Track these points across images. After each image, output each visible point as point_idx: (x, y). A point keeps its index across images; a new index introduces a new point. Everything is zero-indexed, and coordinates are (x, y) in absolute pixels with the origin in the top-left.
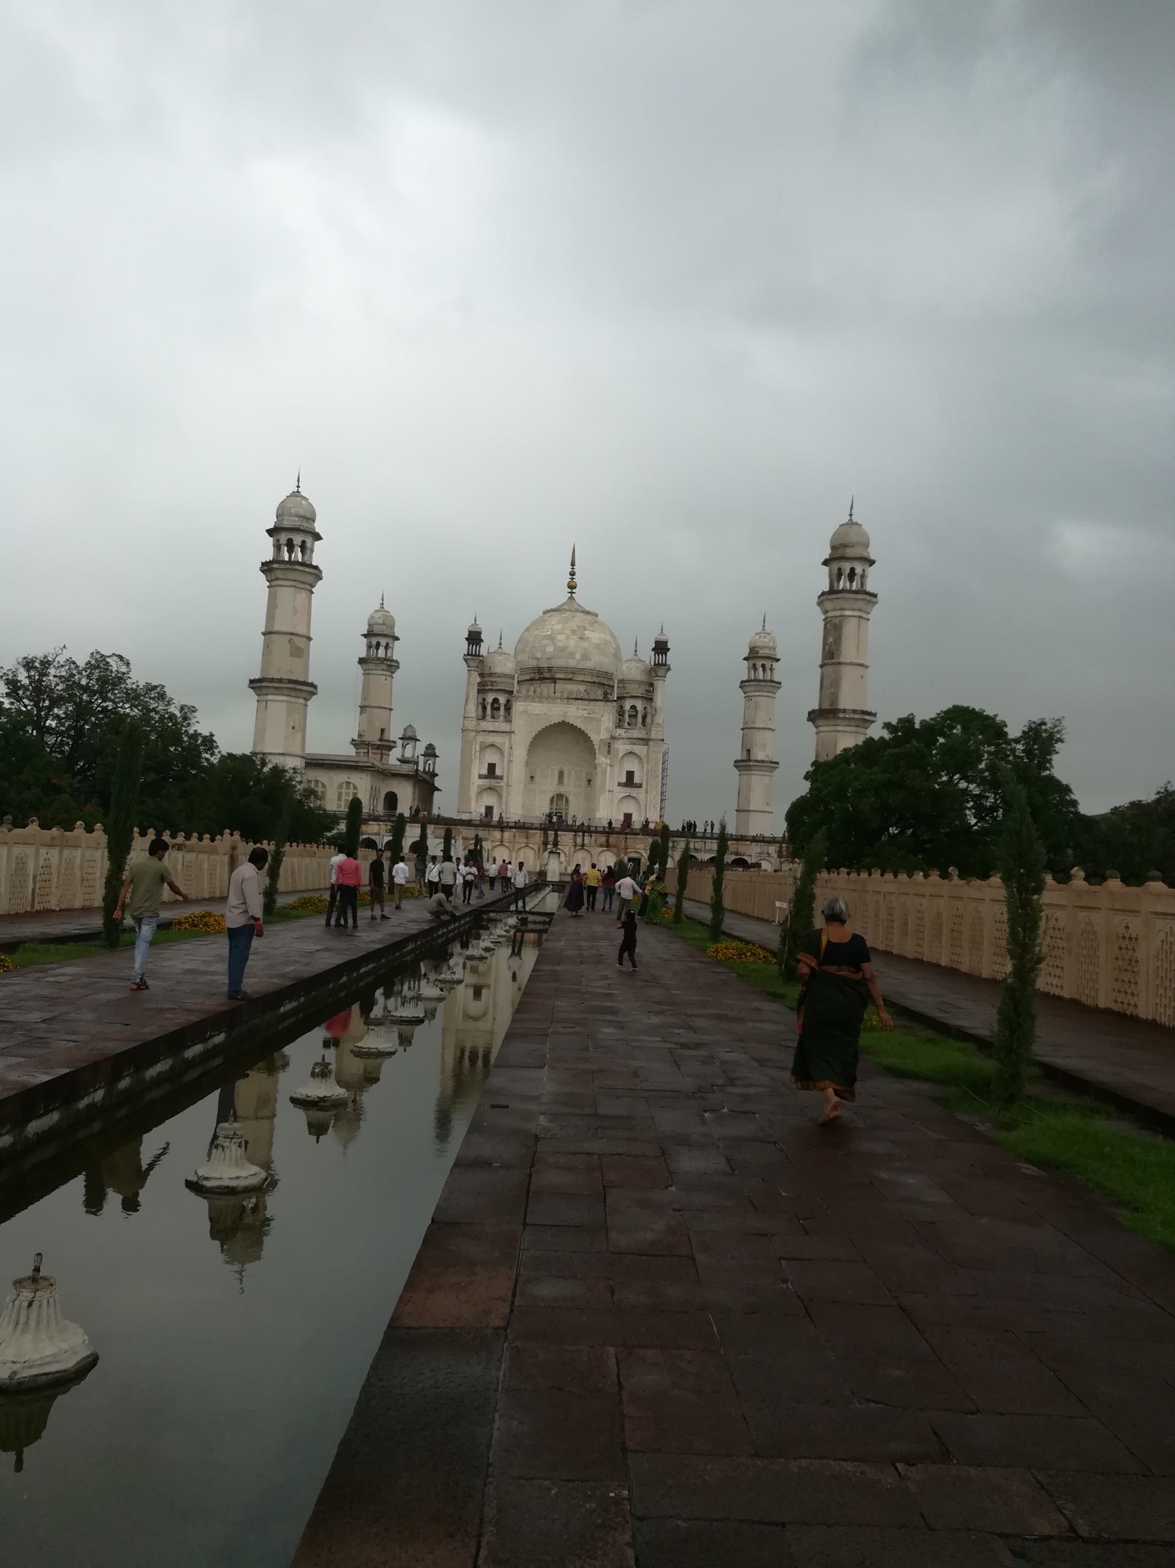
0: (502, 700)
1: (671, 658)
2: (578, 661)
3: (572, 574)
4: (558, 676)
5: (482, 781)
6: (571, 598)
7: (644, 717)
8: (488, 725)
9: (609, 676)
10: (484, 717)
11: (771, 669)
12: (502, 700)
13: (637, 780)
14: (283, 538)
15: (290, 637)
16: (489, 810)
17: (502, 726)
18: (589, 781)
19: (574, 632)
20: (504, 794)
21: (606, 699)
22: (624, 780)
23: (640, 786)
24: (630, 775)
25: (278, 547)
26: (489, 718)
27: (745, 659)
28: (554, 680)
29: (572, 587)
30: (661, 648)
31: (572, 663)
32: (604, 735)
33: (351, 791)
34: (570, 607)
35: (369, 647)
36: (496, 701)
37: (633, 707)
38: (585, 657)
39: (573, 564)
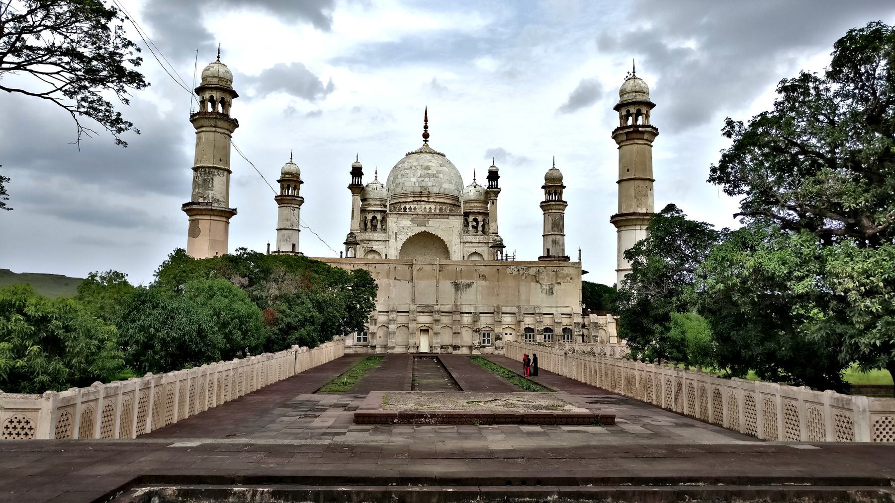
0: (379, 217)
1: (501, 183)
3: (426, 127)
6: (426, 145)
9: (456, 199)
11: (561, 194)
12: (379, 217)
14: (207, 95)
17: (377, 236)
25: (203, 103)
26: (369, 230)
27: (543, 187)
29: (426, 136)
30: (493, 176)
34: (426, 150)
35: (282, 188)
36: (374, 218)
39: (426, 120)
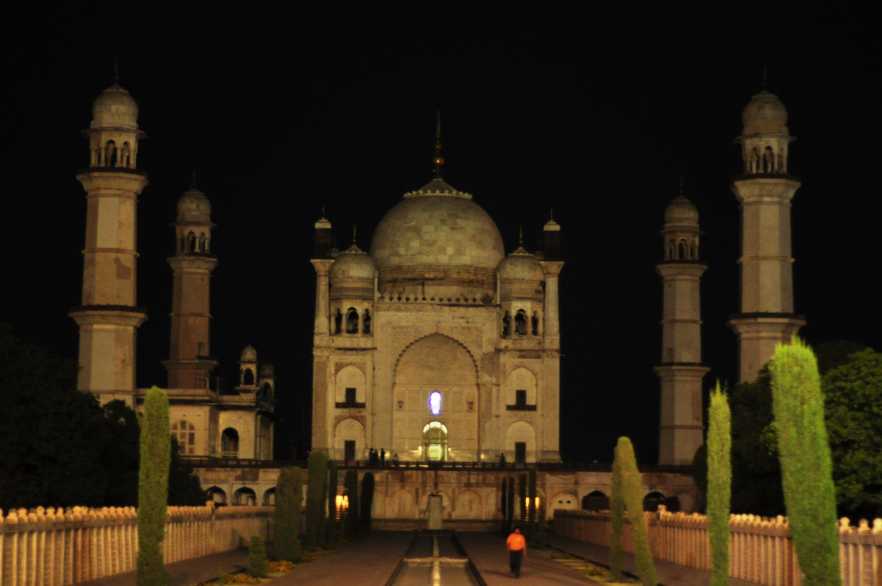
0: (360, 311)
2: (451, 257)
4: (427, 276)
5: (339, 412)
7: (535, 321)
8: (344, 340)
10: (338, 331)
13: (530, 401)
15: (114, 255)
16: (350, 446)
18: (471, 404)
19: (443, 222)
20: (369, 424)
21: (487, 302)
22: (512, 401)
23: (533, 408)
24: (521, 395)
28: (422, 281)
31: (444, 259)
32: (488, 348)
33: (187, 431)
37: (521, 311)
38: (459, 252)
